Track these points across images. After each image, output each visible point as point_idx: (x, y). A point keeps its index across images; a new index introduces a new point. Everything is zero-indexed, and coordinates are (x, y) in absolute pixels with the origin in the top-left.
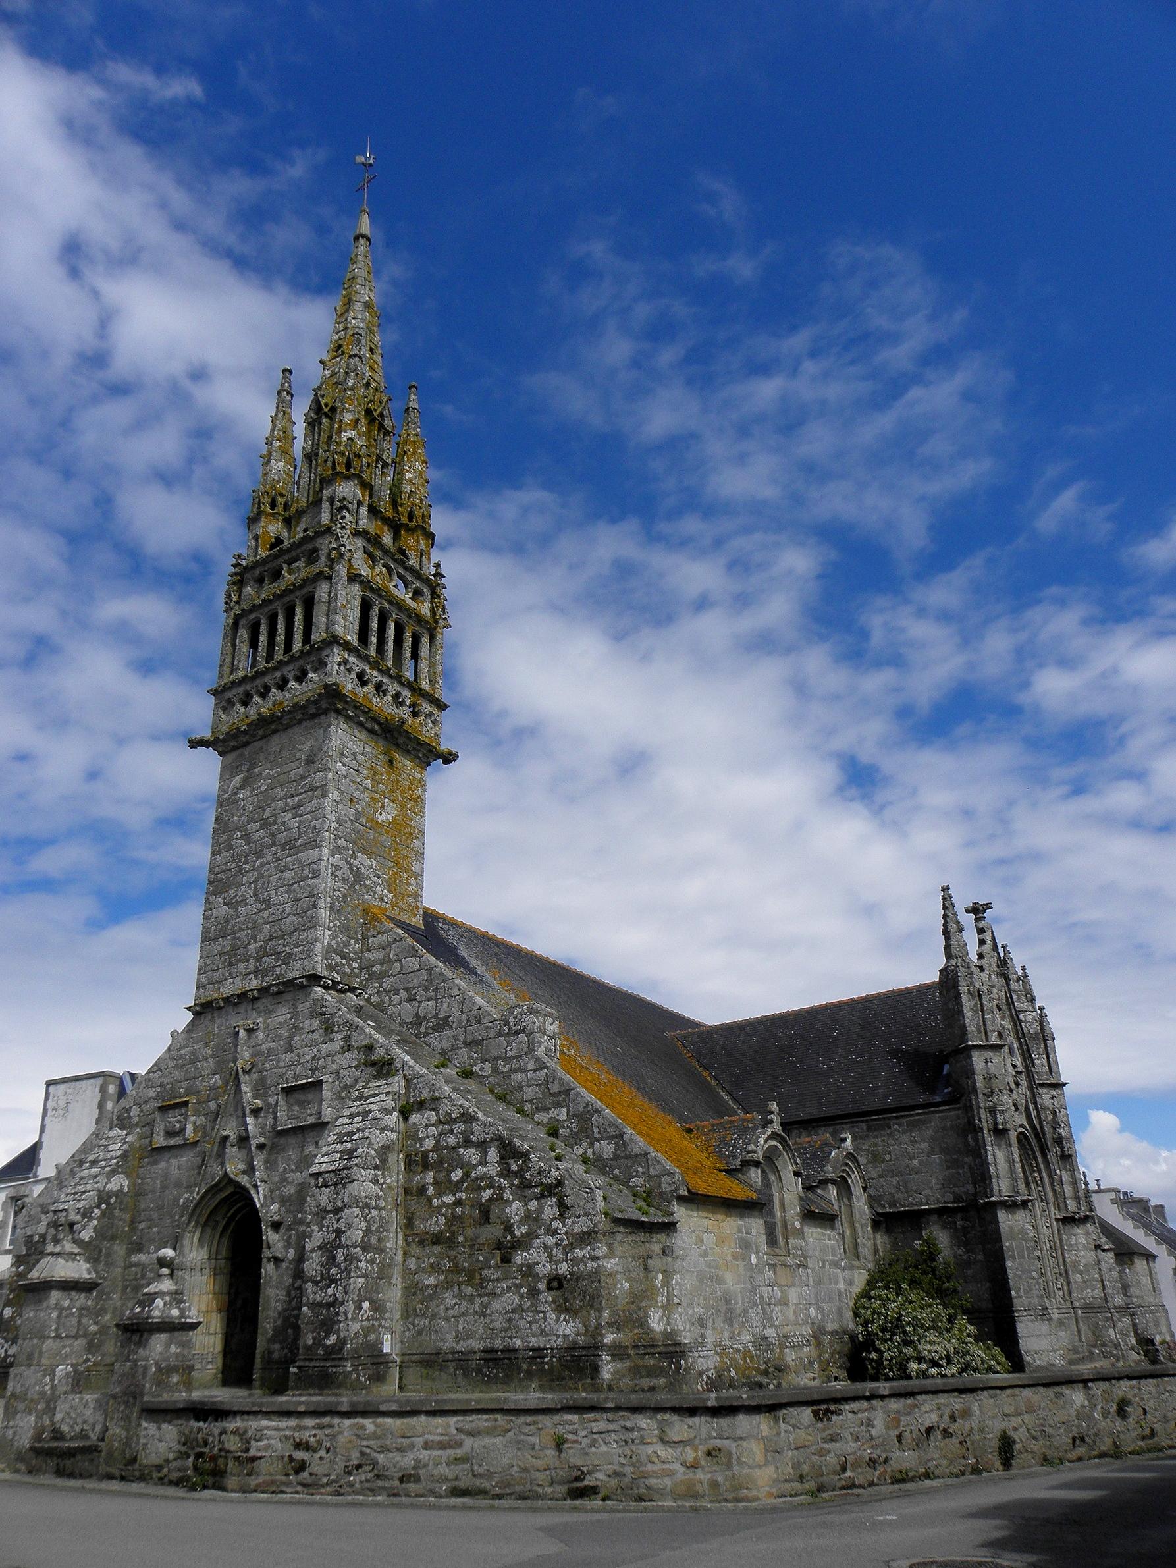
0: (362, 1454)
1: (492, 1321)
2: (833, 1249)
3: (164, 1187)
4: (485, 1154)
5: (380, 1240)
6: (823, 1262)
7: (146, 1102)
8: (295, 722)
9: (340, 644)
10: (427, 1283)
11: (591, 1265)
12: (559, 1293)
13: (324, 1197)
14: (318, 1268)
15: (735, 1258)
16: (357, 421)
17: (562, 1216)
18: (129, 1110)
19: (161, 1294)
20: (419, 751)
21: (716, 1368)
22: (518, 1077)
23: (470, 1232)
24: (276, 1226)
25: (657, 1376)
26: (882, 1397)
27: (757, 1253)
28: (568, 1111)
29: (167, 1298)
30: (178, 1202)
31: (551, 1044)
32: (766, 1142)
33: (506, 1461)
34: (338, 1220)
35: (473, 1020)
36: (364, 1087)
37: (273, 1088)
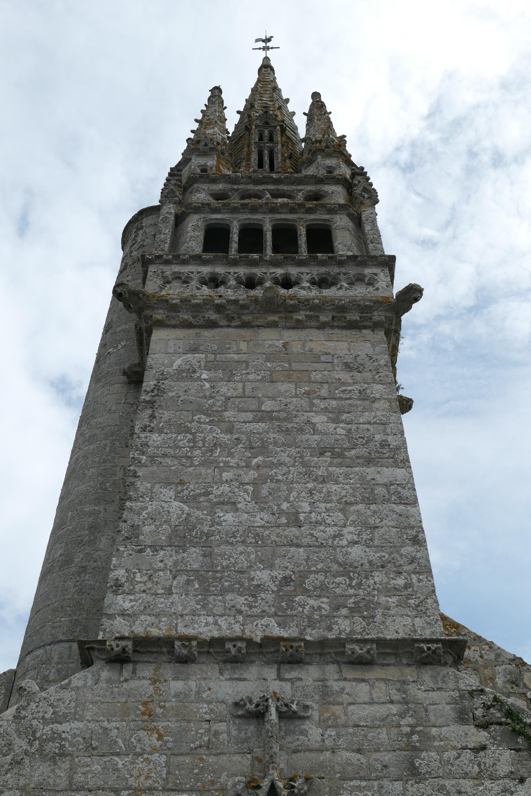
8: (314, 323)
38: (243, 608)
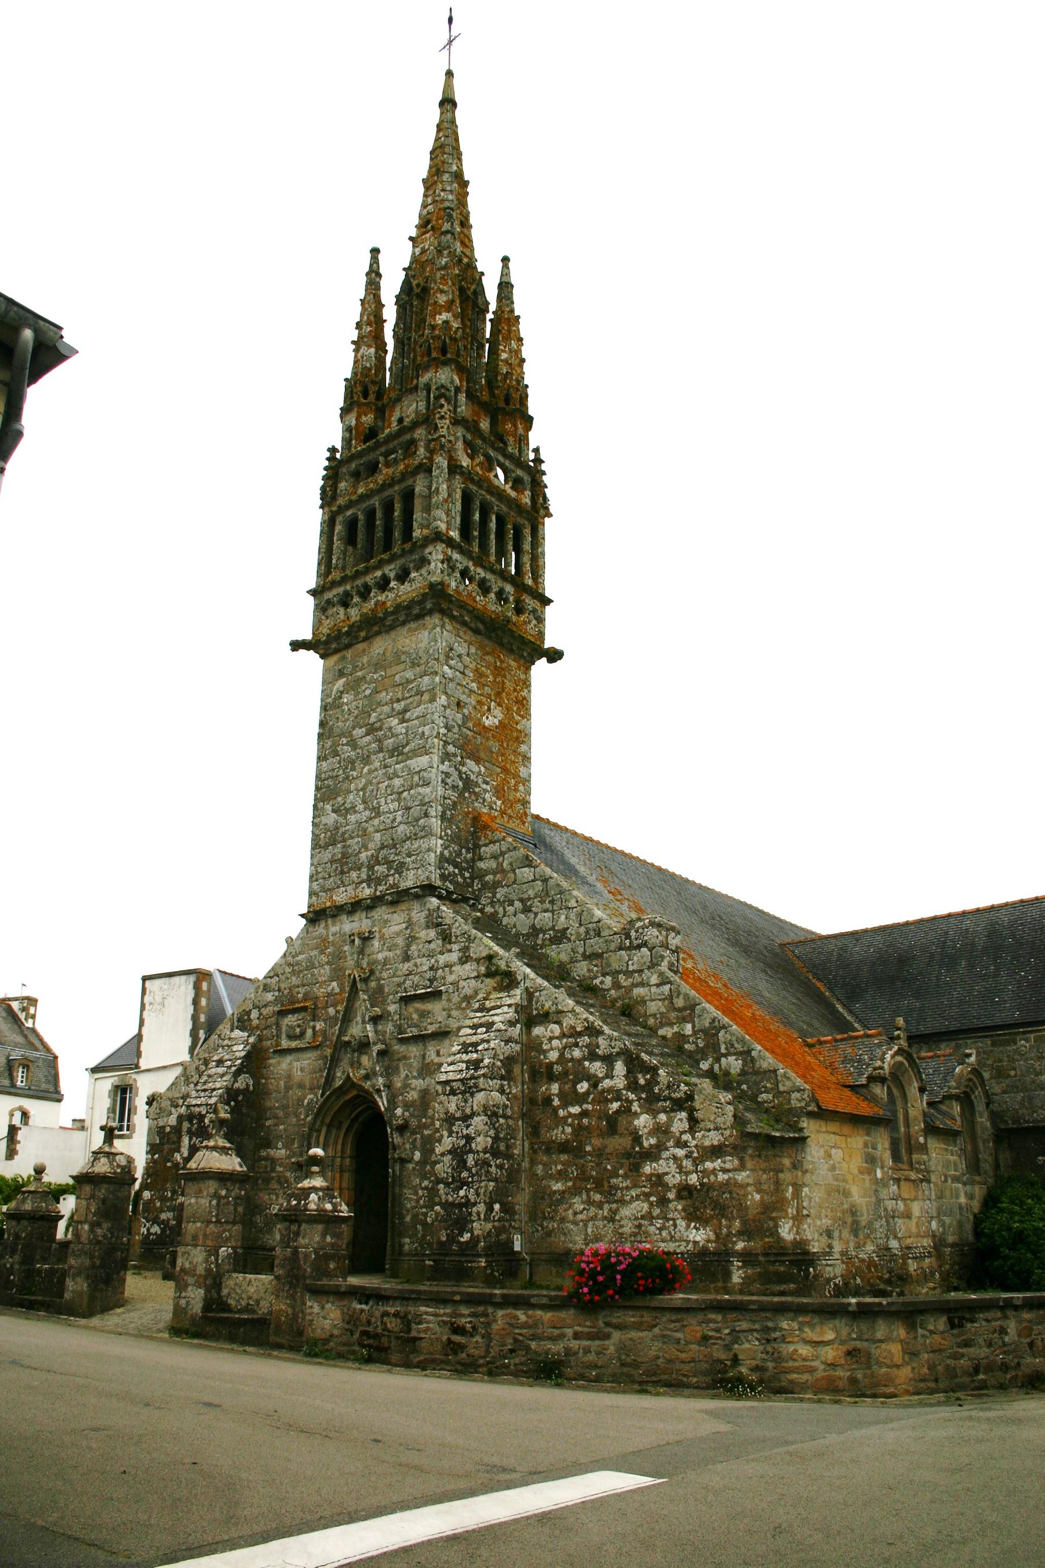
0: (516, 1340)
1: (622, 1226)
2: (955, 1164)
3: (288, 1088)
4: (611, 1067)
5: (508, 1147)
6: (946, 1177)
7: (265, 1006)
9: (443, 541)
10: (554, 1188)
11: (722, 1177)
12: (689, 1202)
13: (452, 1105)
14: (450, 1170)
15: (861, 1173)
16: (452, 302)
17: (692, 1130)
18: (249, 1013)
19: (314, 1189)
20: (523, 650)
21: (842, 1276)
22: (639, 991)
23: (597, 1142)
24: (402, 1129)
25: (786, 1282)
26: (1016, 1308)
27: (882, 1168)
28: (693, 1027)
29: (321, 1194)
30: (303, 1101)
31: (674, 959)
32: (893, 1057)
33: (652, 1353)
34: (468, 1127)
35: (592, 933)
36: (485, 999)
37: (391, 997)
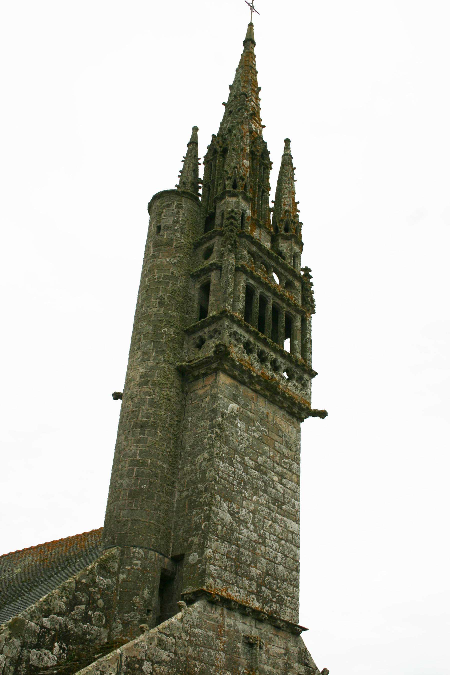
8: (279, 404)
18: (141, 662)
38: (247, 587)
